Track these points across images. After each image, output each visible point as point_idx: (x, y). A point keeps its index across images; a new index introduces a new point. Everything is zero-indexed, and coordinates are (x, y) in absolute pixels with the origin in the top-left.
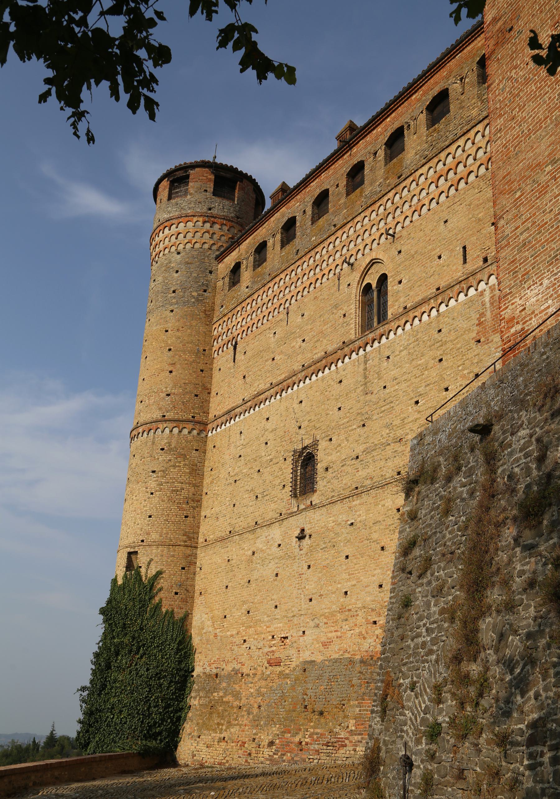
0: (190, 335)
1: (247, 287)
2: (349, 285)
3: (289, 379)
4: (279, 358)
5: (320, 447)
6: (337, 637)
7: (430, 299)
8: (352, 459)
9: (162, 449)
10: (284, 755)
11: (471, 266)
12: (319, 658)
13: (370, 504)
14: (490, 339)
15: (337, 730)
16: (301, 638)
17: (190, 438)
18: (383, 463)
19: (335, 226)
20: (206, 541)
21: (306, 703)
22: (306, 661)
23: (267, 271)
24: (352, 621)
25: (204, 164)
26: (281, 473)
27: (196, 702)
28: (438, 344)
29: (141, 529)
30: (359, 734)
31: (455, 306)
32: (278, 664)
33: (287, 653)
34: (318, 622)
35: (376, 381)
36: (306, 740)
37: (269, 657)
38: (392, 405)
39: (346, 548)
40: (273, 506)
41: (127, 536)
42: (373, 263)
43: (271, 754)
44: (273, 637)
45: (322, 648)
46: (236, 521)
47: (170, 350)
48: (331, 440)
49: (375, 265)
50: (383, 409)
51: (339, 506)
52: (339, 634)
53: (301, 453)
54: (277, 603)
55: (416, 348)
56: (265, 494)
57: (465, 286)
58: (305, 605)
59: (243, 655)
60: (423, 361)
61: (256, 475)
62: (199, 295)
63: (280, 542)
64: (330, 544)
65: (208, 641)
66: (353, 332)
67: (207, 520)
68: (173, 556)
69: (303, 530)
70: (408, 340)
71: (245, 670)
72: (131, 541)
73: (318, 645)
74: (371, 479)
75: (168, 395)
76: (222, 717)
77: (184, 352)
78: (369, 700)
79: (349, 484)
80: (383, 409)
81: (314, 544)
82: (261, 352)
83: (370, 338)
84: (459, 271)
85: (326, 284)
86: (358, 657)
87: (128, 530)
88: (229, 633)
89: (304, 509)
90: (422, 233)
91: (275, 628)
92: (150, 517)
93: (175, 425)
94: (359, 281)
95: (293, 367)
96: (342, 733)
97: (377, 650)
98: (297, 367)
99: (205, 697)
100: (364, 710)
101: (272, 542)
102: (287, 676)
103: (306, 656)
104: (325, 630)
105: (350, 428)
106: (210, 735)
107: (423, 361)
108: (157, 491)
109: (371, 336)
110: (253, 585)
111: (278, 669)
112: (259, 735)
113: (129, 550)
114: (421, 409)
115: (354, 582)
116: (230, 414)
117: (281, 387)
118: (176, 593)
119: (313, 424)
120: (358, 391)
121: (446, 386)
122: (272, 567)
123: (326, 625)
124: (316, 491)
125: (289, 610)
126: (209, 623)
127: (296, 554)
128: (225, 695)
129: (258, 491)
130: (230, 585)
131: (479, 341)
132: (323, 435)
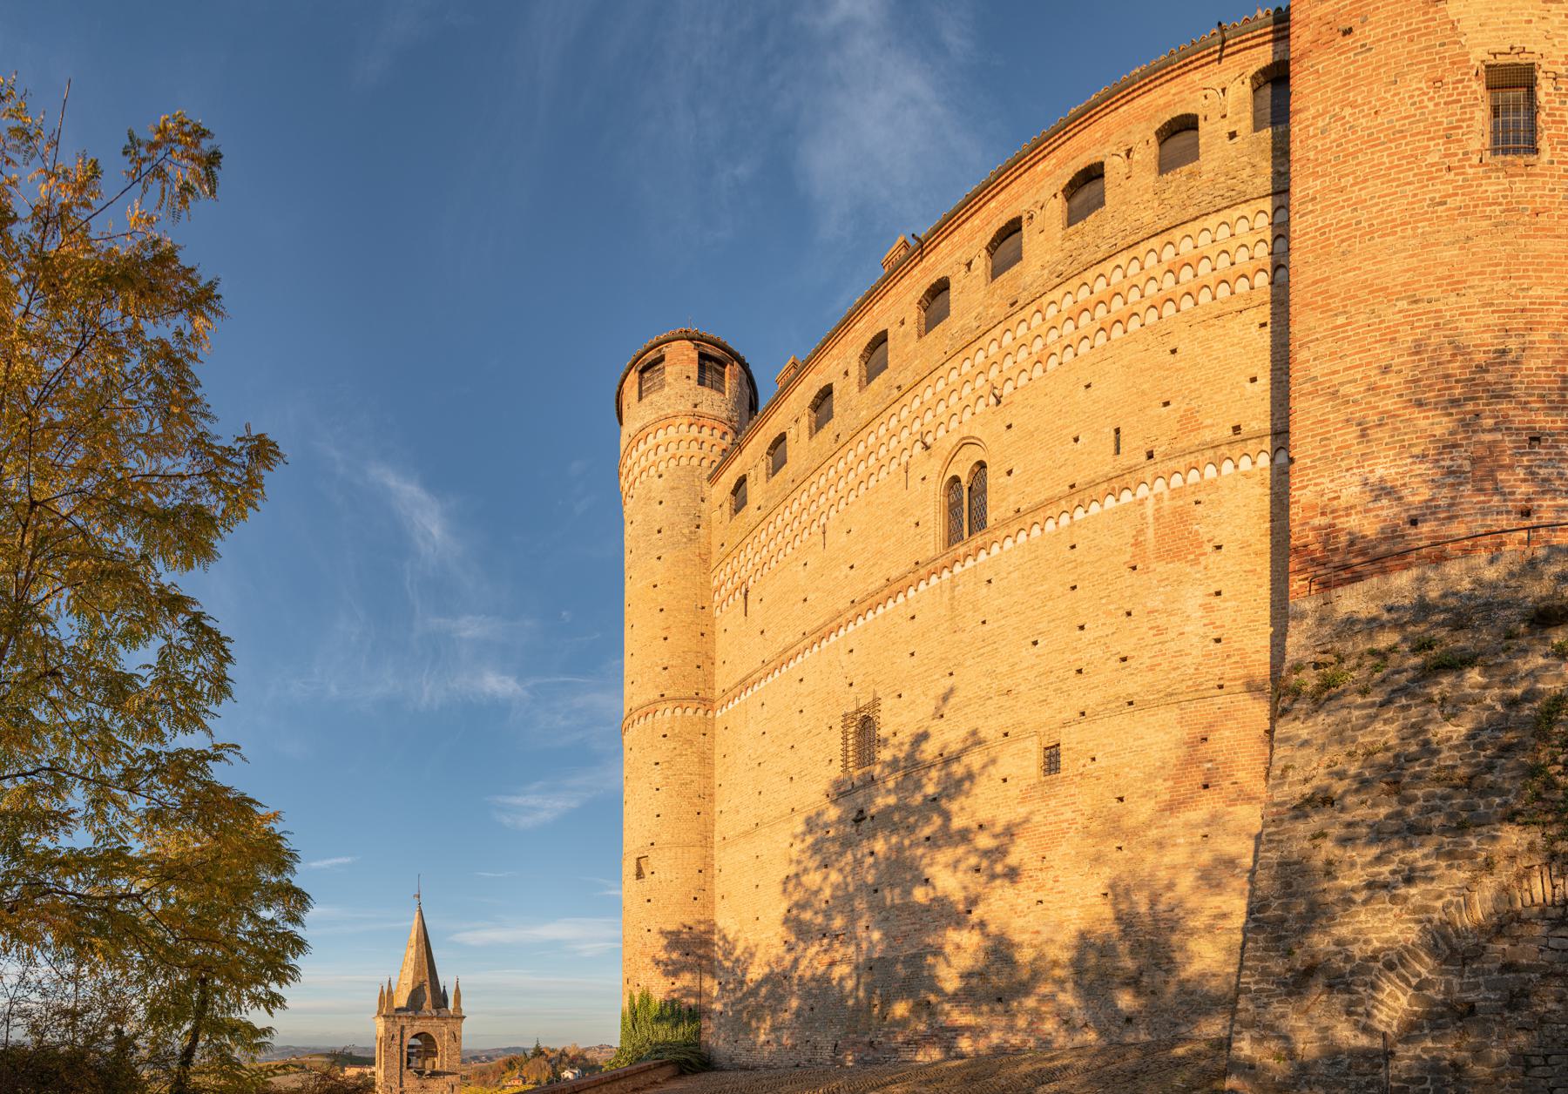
14: (1152, 567)
42: (965, 442)
109: (962, 550)
131: (1134, 568)
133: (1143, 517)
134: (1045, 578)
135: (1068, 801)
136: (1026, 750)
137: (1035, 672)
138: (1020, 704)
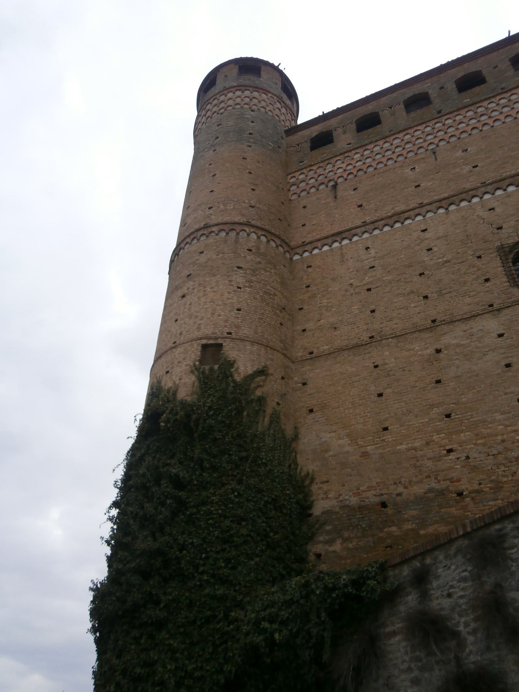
9: (250, 250)
25: (275, 69)
27: (337, 547)
29: (226, 321)
40: (467, 300)
68: (272, 360)
71: (464, 486)
88: (403, 447)
93: (263, 233)
108: (246, 286)
113: (204, 342)
126: (346, 441)
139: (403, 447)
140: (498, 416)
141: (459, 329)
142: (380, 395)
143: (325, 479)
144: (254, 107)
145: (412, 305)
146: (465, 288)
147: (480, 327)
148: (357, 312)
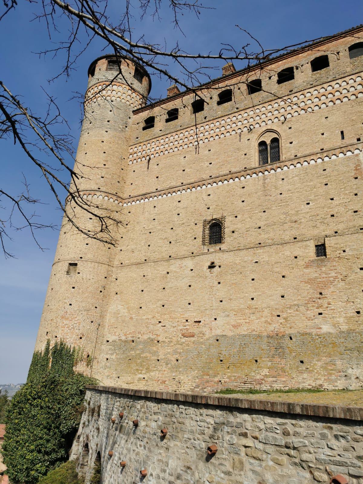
0: (117, 148)
1: (161, 130)
2: (249, 140)
3: (199, 182)
4: (189, 170)
5: (226, 220)
6: (246, 323)
7: (317, 153)
8: (255, 228)
10: (205, 388)
11: (347, 141)
12: (230, 334)
13: (272, 252)
15: (253, 375)
16: (213, 323)
17: (114, 204)
18: (281, 232)
19: (237, 108)
20: (122, 264)
21: (221, 359)
22: (218, 335)
23: (179, 124)
24: (258, 315)
26: (192, 231)
28: (324, 176)
29: (80, 251)
30: (273, 377)
31: (336, 159)
32: (193, 336)
33: (200, 330)
34: (229, 314)
35: (274, 190)
36: (224, 380)
37: (184, 332)
38: (287, 203)
39: (252, 275)
40: (185, 248)
41: (68, 254)
43: (193, 388)
44: (187, 321)
45: (232, 328)
46: (151, 254)
47: (104, 153)
48: (236, 217)
49: (268, 133)
50: (280, 204)
51: (244, 252)
52: (247, 321)
53: (210, 222)
54: (190, 302)
55: (305, 177)
56: (178, 241)
57: (345, 150)
58: (216, 304)
59: (158, 330)
60: (312, 183)
61: (170, 231)
62: (123, 128)
63: (193, 268)
64: (238, 272)
65: (123, 321)
66: (253, 163)
67: (122, 252)
69: (213, 263)
70: (299, 172)
71: (160, 338)
72: (72, 257)
73: (228, 327)
74: (273, 239)
75: (102, 177)
76: (142, 365)
77: (113, 156)
78: (279, 358)
79: (253, 241)
80: (280, 204)
81: (223, 271)
82: (172, 165)
83: (269, 168)
84: (339, 143)
85: (228, 137)
86: (265, 334)
87: (69, 250)
88: (144, 317)
89: (213, 252)
90: (308, 121)
91: (188, 316)
92: (87, 244)
93: (106, 195)
94: (257, 139)
95: (202, 176)
96: (258, 376)
97: (281, 330)
98: (205, 176)
99: (123, 354)
100: (274, 364)
101: (184, 268)
102: (202, 343)
103: (219, 332)
104: (234, 318)
105: (253, 212)
106: (130, 376)
107: (312, 183)
109: (269, 167)
110: (167, 291)
111: (192, 339)
112: (179, 376)
113: (70, 262)
114: (311, 207)
115: (260, 293)
116: (145, 196)
117: (193, 185)
118: (101, 292)
119: (220, 207)
120: (259, 194)
121: (331, 198)
122: (187, 281)
123: (235, 316)
124: (224, 243)
125: (202, 306)
126: (126, 311)
127: (207, 275)
128: (143, 352)
129: (171, 240)
130: (145, 290)
132: (230, 214)
133: (358, 160)
134: (311, 181)
135: (332, 268)
136: (307, 246)
137: (309, 215)
138: (302, 227)
139: (144, 317)
140: (180, 310)
141: (178, 262)
142: (142, 291)
143: (116, 327)
144: (113, 99)
145: (164, 246)
146: (186, 241)
147: (185, 264)
148: (143, 245)
